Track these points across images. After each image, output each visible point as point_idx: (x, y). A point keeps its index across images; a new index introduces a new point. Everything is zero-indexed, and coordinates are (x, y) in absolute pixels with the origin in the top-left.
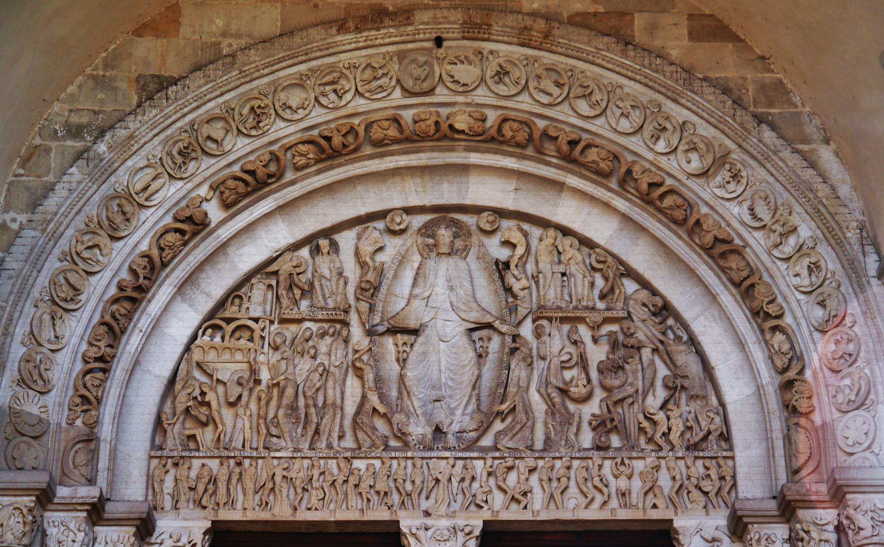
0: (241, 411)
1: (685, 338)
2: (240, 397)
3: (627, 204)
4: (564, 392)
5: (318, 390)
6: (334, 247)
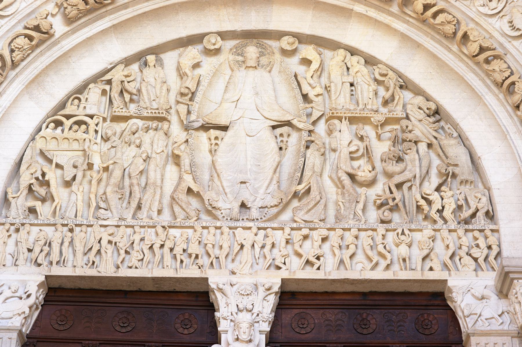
0: (74, 187)
1: (455, 134)
2: (74, 178)
3: (405, 25)
4: (352, 177)
5: (141, 172)
6: (160, 62)
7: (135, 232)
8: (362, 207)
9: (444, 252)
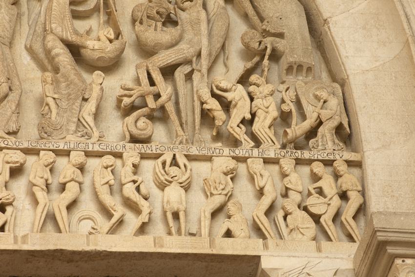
8: (94, 110)
9: (254, 201)
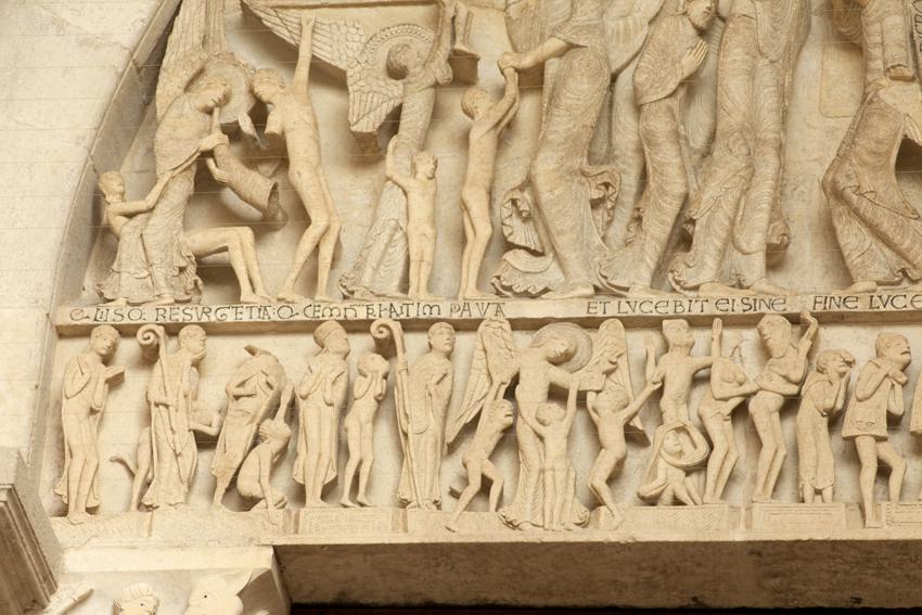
7: (666, 348)
